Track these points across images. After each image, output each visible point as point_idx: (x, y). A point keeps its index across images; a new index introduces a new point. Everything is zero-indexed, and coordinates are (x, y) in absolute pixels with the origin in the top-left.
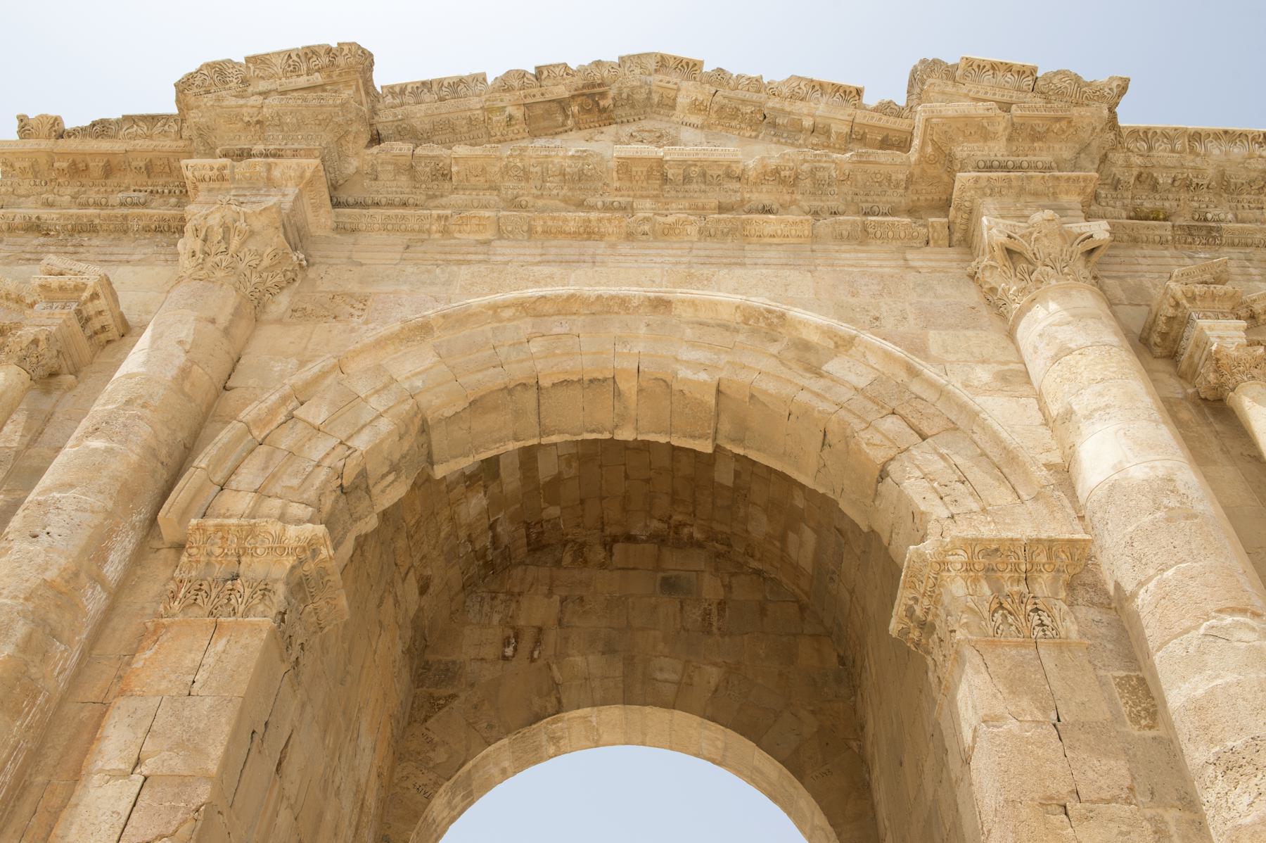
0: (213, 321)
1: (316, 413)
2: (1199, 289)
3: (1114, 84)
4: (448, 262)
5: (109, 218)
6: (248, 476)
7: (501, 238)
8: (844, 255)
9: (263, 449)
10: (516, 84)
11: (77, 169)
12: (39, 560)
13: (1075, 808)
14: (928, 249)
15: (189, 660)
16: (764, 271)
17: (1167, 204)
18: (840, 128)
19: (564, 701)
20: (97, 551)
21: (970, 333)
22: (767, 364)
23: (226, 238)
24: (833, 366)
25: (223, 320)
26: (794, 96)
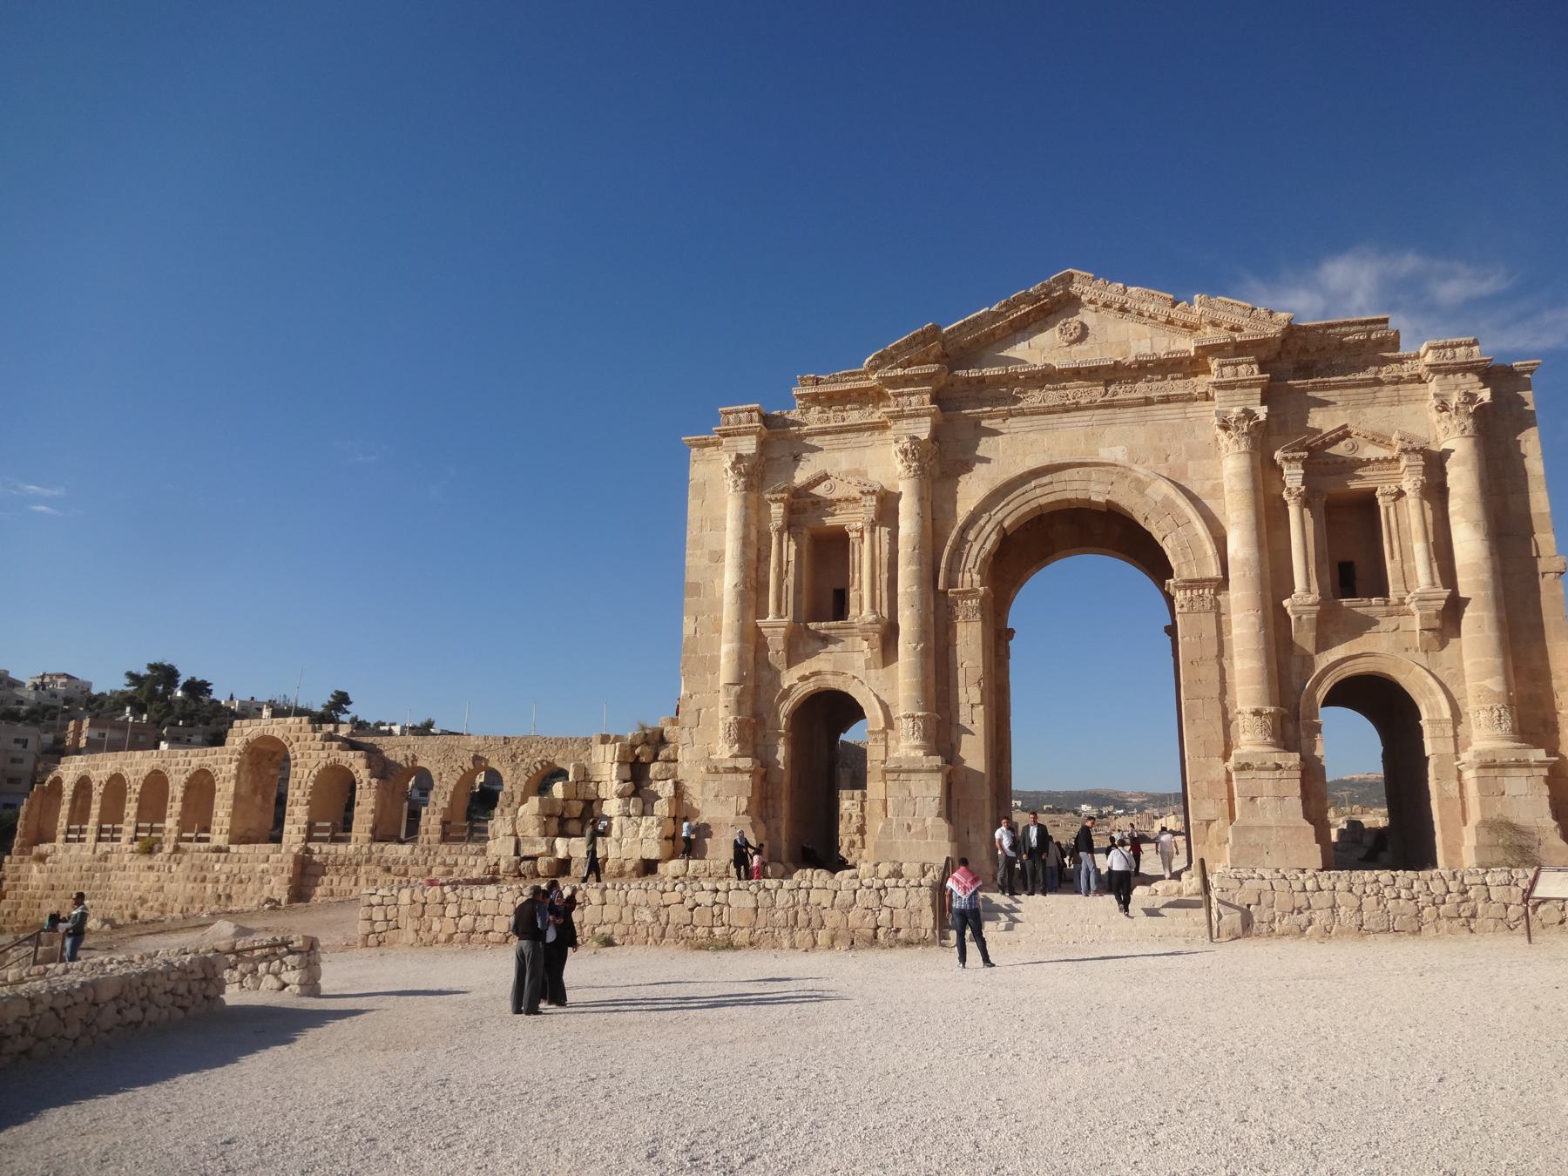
2: (1290, 455)
8: (1159, 412)
13: (1200, 663)
17: (1314, 358)
21: (1205, 462)
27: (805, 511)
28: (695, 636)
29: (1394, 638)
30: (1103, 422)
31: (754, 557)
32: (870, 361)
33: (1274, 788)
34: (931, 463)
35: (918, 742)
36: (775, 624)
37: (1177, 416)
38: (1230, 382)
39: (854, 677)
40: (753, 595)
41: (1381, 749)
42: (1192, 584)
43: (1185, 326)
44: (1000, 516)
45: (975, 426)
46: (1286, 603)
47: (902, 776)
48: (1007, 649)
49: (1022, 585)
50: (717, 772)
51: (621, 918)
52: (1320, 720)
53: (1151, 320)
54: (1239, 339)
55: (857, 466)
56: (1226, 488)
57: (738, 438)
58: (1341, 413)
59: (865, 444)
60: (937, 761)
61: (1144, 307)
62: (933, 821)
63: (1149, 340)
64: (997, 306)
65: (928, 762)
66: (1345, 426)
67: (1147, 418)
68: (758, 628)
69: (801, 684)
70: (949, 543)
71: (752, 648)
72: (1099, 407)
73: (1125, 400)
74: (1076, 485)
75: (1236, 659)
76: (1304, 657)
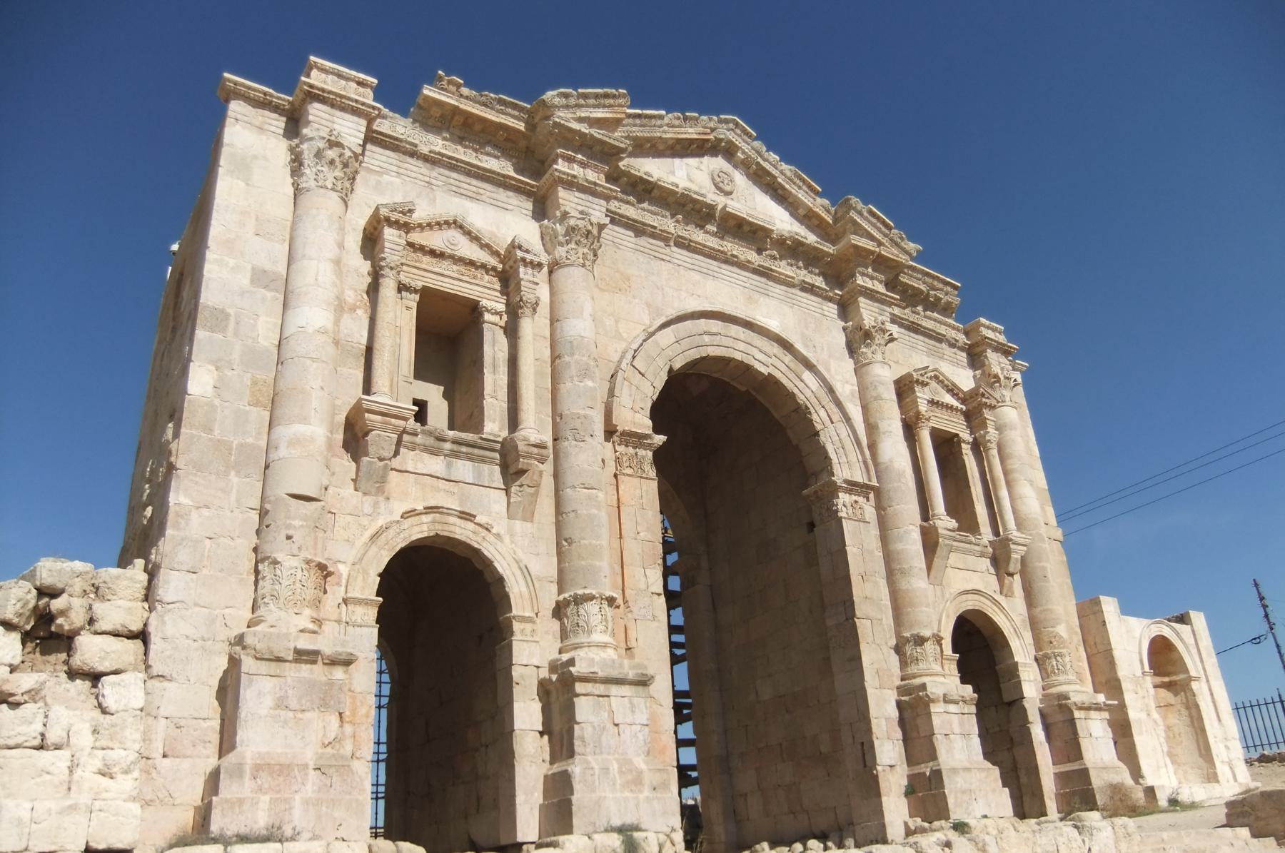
2: (921, 378)
9: (626, 382)
15: (638, 492)
22: (783, 368)
30: (757, 289)
32: (553, 97)
35: (606, 638)
36: (392, 411)
37: (816, 310)
42: (853, 487)
43: (818, 226)
44: (670, 353)
47: (600, 689)
50: (279, 660)
54: (883, 252)
55: (494, 229)
57: (338, 113)
59: (505, 205)
61: (792, 189)
64: (670, 115)
65: (632, 668)
67: (794, 302)
69: (407, 523)
72: (755, 271)
73: (780, 273)
74: (741, 346)
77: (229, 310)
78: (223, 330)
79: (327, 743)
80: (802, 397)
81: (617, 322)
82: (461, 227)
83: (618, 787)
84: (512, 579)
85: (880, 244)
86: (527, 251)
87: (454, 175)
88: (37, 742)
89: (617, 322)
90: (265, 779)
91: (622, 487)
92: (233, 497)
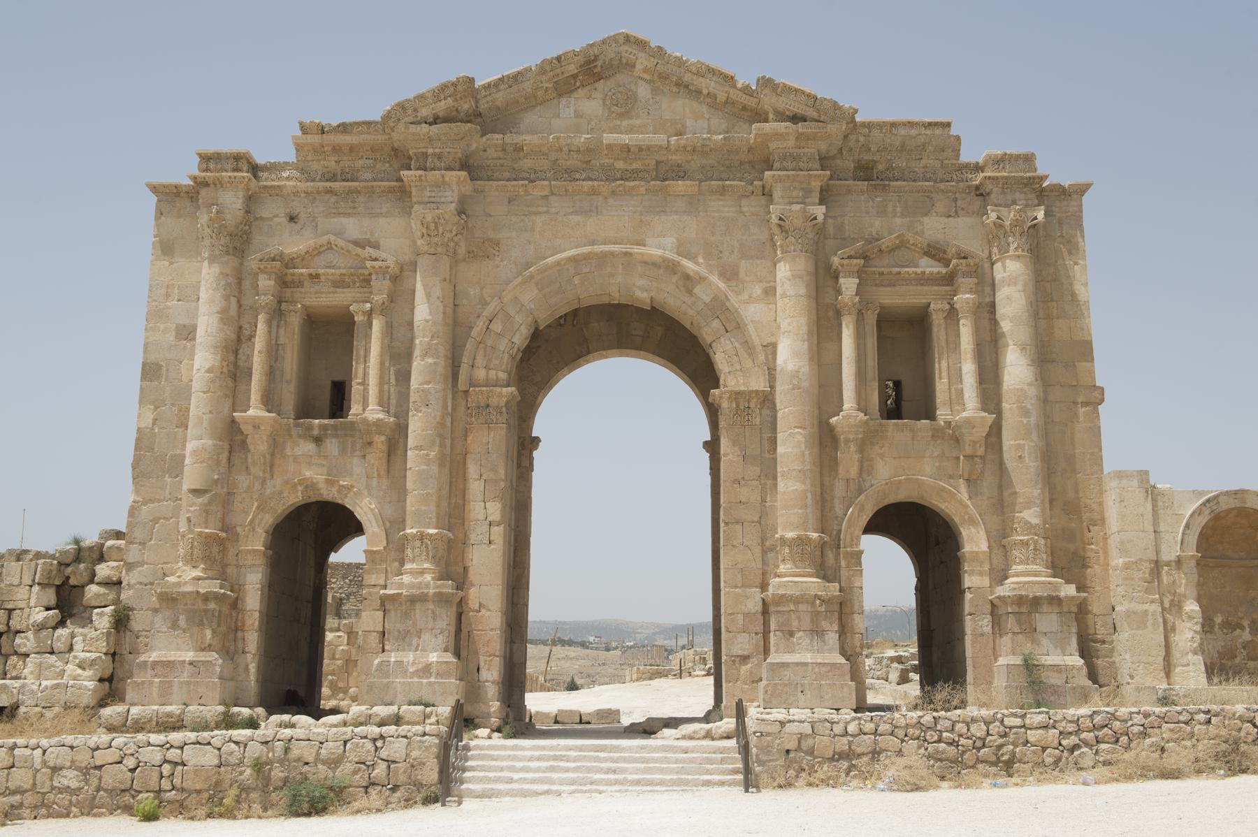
0: (445, 280)
1: (497, 326)
3: (851, 111)
4: (530, 213)
5: (365, 187)
6: (480, 361)
7: (553, 194)
8: (713, 204)
9: (481, 346)
10: (548, 68)
11: (336, 149)
12: (433, 415)
13: (742, 482)
14: (752, 198)
16: (675, 217)
18: (721, 97)
19: (590, 348)
20: (445, 406)
21: (758, 262)
23: (437, 228)
24: (697, 290)
25: (448, 278)
26: (698, 74)
27: (301, 284)
28: (152, 429)
29: (937, 464)
31: (234, 336)
33: (812, 621)
34: (456, 239)
38: (788, 176)
39: (352, 486)
40: (230, 382)
41: (913, 580)
42: (737, 395)
45: (509, 202)
46: (834, 420)
48: (531, 460)
49: (551, 388)
51: (34, 784)
52: (861, 547)
53: (708, 100)
56: (779, 291)
58: (898, 221)
60: (448, 587)
62: (439, 657)
63: (706, 121)
66: (902, 235)
68: (233, 421)
70: (474, 333)
71: (228, 446)
75: (779, 480)
76: (847, 480)
77: (162, 363)
78: (159, 378)
79: (203, 646)
80: (691, 312)
81: (482, 289)
82: (336, 246)
83: (409, 674)
84: (368, 523)
85: (796, 119)
86: (376, 260)
87: (333, 199)
88: (49, 650)
89: (482, 289)
90: (159, 669)
91: (470, 439)
92: (167, 492)
